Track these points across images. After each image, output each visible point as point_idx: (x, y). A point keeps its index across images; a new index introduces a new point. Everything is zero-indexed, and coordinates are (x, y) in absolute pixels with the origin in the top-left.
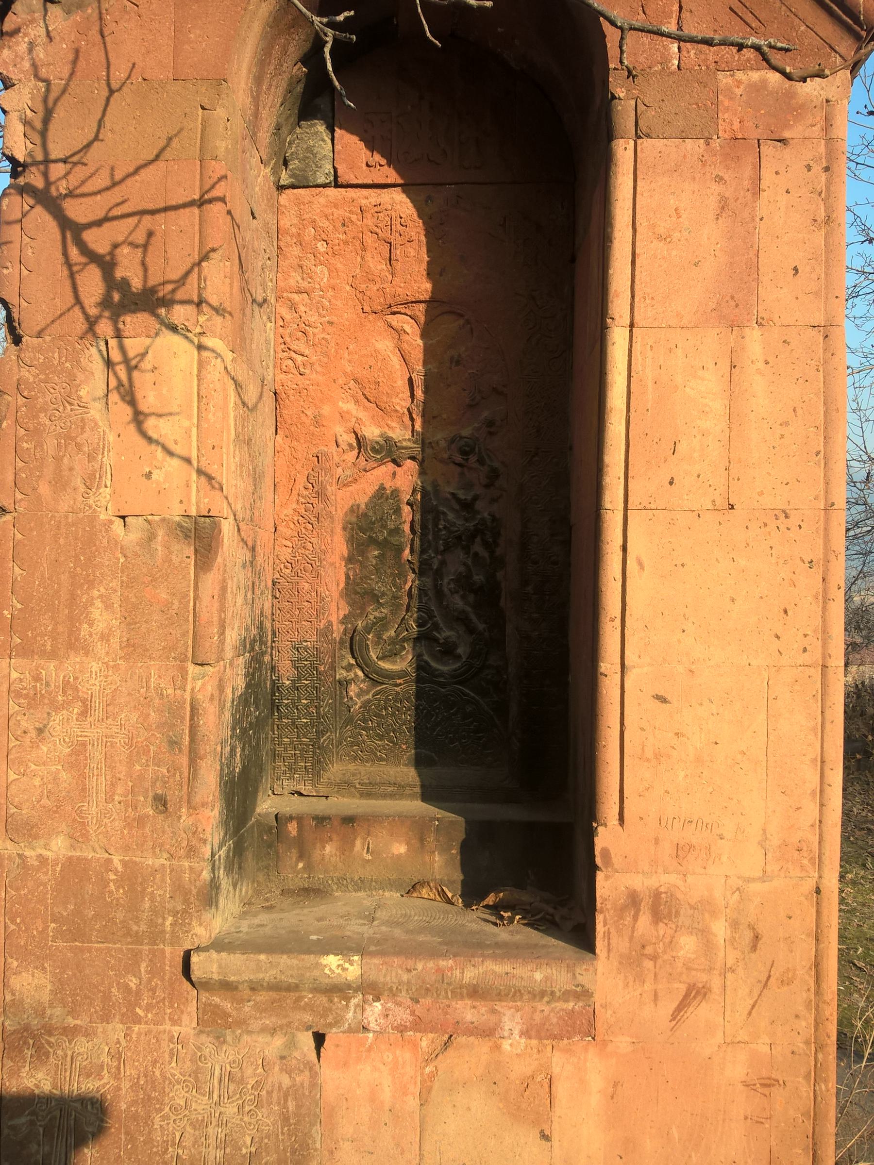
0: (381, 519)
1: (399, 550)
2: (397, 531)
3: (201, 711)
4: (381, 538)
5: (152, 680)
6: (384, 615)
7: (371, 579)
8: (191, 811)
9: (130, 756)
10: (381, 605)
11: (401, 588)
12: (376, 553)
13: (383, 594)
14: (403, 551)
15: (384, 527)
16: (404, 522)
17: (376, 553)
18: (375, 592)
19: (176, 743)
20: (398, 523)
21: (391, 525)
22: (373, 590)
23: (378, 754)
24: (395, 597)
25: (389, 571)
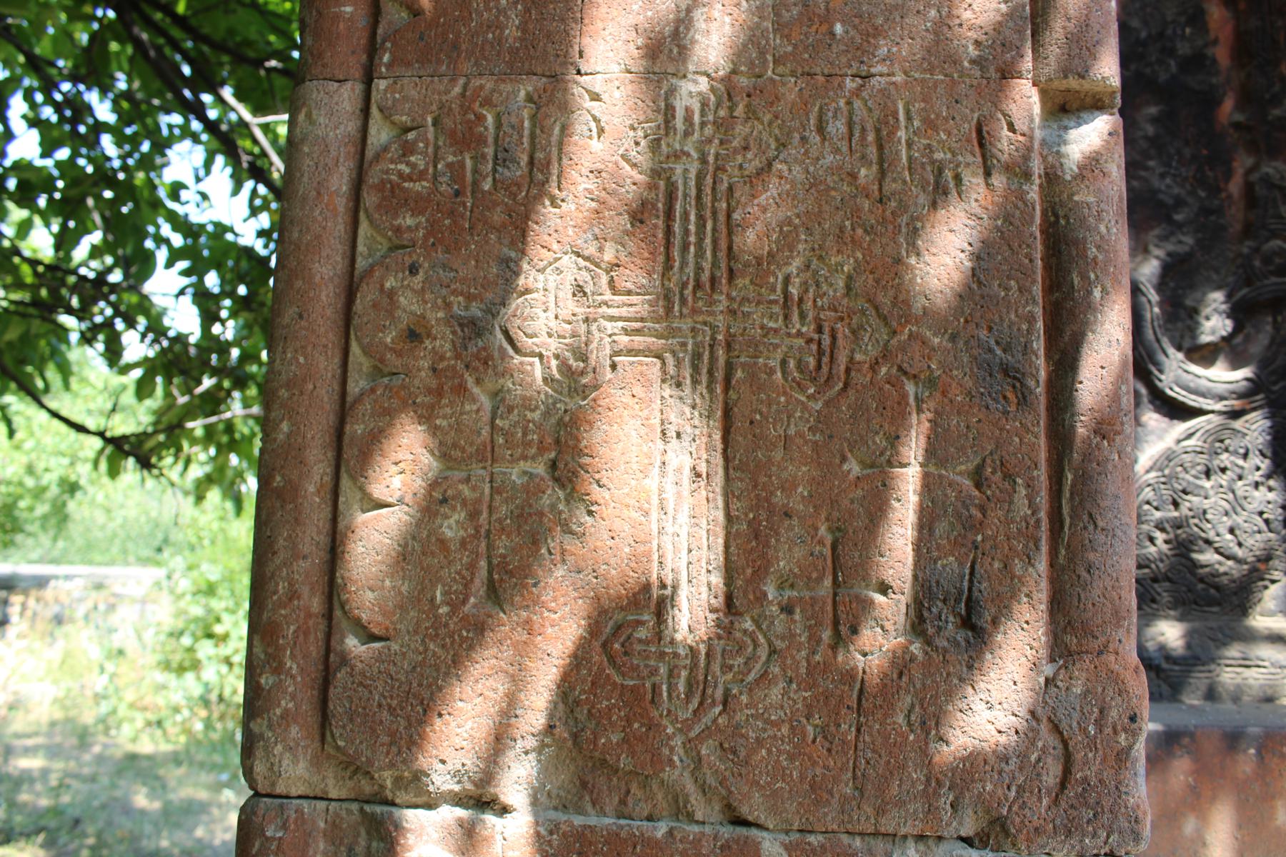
0: (1161, 35)
1: (1210, 101)
2: (1198, 62)
3: (1093, 251)
4: (1163, 77)
5: (902, 134)
6: (1187, 249)
7: (1147, 169)
8: (1071, 640)
9: (822, 422)
10: (1180, 226)
11: (1219, 190)
12: (1153, 110)
13: (1179, 203)
14: (1219, 103)
15: (1171, 52)
16: (1215, 42)
17: (1153, 110)
18: (1161, 196)
19: (1006, 370)
20: (1200, 43)
21: (1183, 49)
22: (1156, 192)
23: (1200, 586)
24: (1206, 211)
25: (1187, 152)
